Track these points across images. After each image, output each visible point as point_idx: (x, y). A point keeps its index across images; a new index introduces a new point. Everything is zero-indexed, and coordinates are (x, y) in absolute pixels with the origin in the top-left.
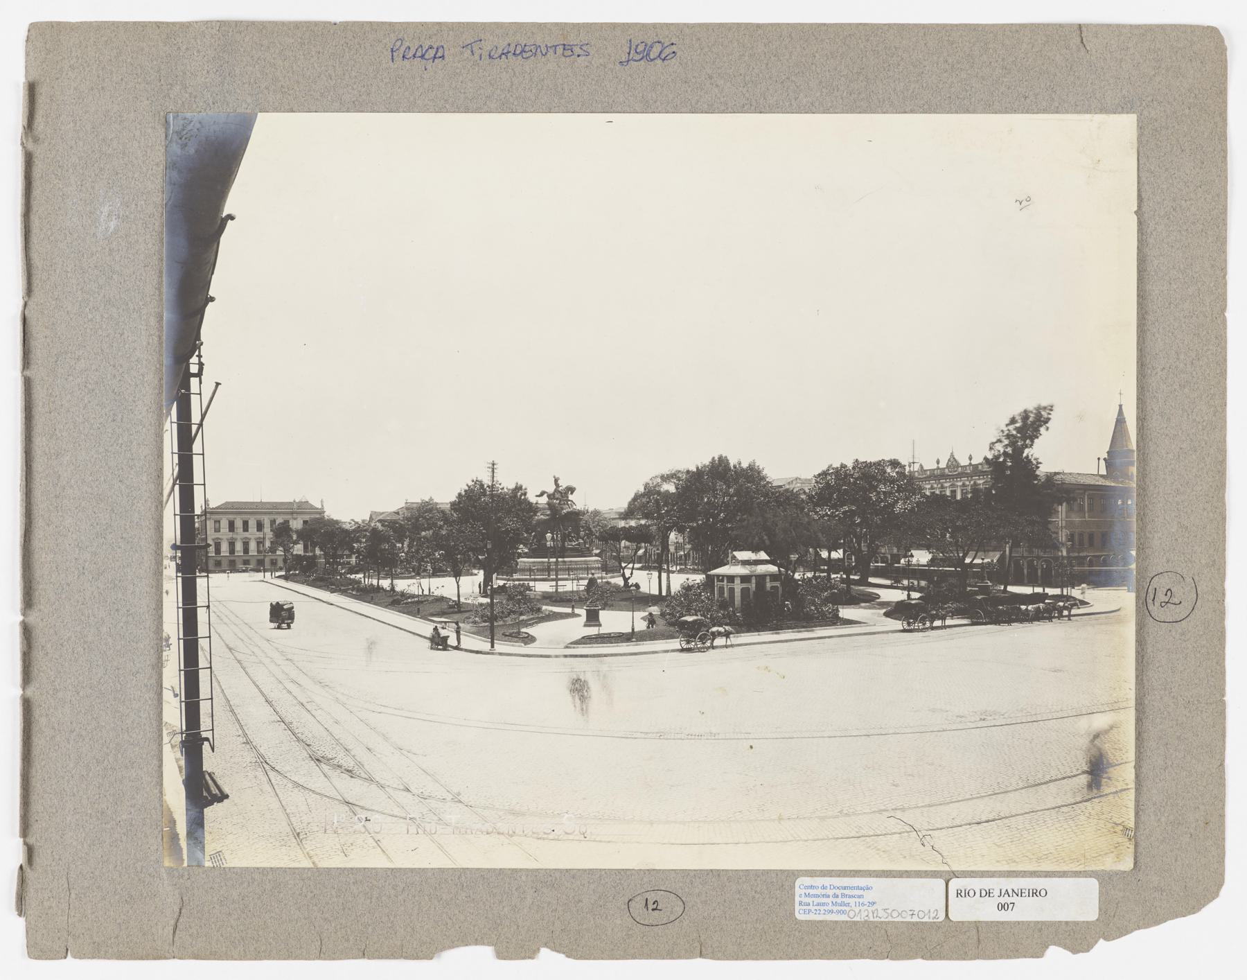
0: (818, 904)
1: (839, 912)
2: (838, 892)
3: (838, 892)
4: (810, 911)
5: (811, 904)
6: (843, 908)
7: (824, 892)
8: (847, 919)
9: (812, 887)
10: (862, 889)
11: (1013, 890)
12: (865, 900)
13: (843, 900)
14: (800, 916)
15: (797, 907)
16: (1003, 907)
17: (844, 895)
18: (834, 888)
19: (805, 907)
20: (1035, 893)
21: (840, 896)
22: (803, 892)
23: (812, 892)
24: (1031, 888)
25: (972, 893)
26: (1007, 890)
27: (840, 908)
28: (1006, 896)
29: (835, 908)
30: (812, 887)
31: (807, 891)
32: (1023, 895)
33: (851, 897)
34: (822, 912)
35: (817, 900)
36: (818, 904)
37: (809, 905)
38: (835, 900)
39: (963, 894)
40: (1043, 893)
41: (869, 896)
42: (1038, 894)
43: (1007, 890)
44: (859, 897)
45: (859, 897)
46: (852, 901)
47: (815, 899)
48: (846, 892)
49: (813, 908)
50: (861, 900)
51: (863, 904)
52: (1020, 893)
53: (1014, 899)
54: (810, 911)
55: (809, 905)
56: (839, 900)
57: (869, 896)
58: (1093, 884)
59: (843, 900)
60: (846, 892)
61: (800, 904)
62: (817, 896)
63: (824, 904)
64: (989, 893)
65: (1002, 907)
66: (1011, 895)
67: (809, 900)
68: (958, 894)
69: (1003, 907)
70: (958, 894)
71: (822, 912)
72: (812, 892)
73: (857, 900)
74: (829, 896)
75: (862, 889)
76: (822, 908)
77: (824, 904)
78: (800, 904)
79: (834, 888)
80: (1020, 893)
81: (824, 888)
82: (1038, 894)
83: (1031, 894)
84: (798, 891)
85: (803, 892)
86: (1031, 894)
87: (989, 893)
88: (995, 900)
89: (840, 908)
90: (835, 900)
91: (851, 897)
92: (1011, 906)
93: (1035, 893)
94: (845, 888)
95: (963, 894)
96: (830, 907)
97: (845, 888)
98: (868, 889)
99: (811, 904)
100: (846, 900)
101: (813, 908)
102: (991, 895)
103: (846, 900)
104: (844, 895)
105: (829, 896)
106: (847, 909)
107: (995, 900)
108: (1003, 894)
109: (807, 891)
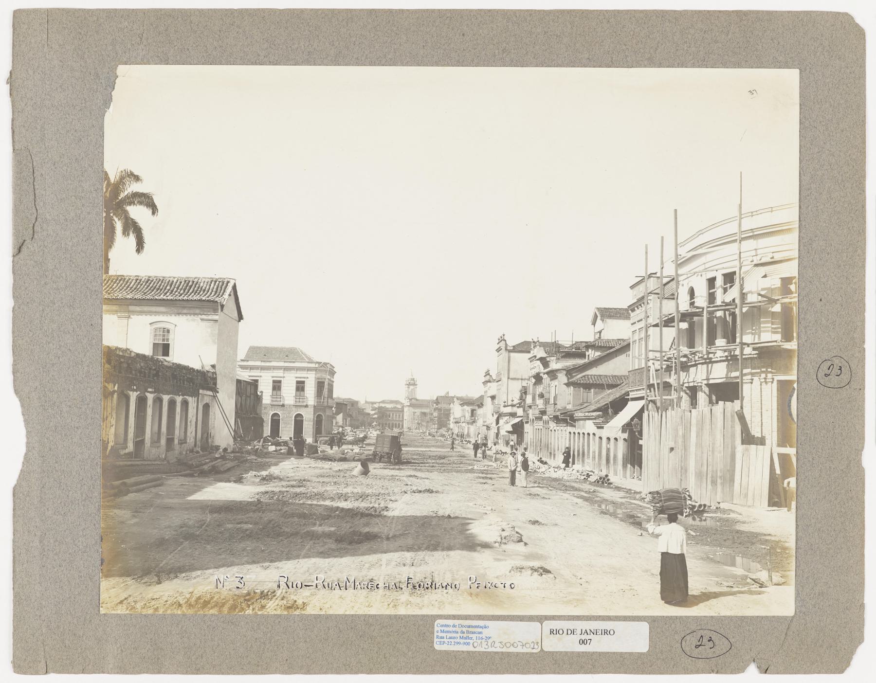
0: (450, 638)
1: (464, 643)
2: (464, 629)
3: (464, 629)
4: (444, 642)
6: (468, 641)
7: (454, 629)
8: (471, 648)
10: (481, 627)
11: (591, 631)
12: (483, 636)
13: (467, 635)
14: (437, 647)
15: (436, 640)
16: (583, 642)
17: (468, 632)
18: (462, 626)
19: (442, 640)
20: (606, 632)
22: (439, 629)
23: (446, 629)
24: (603, 629)
25: (561, 632)
26: (586, 630)
27: (465, 641)
28: (586, 634)
29: (462, 641)
30: (447, 626)
31: (442, 629)
32: (598, 633)
33: (473, 633)
34: (453, 643)
35: (449, 635)
36: (450, 638)
37: (443, 638)
39: (555, 632)
40: (612, 632)
41: (486, 633)
42: (608, 633)
43: (586, 630)
44: (480, 633)
45: (480, 633)
46: (474, 636)
47: (447, 634)
49: (445, 640)
50: (481, 636)
52: (595, 633)
53: (591, 636)
54: (444, 642)
55: (443, 638)
56: (465, 635)
57: (486, 633)
58: (645, 627)
59: (467, 635)
60: (470, 630)
61: (437, 637)
62: (450, 632)
63: (454, 638)
64: (573, 632)
65: (583, 642)
66: (589, 633)
67: (444, 635)
68: (552, 632)
69: (583, 642)
70: (552, 632)
71: (453, 643)
72: (446, 629)
73: (479, 635)
75: (481, 627)
76: (452, 640)
77: (454, 638)
78: (437, 637)
79: (462, 626)
80: (595, 633)
81: (454, 626)
82: (608, 633)
83: (603, 633)
84: (436, 628)
85: (439, 629)
86: (603, 633)
87: (573, 632)
88: (576, 638)
89: (465, 641)
90: (462, 635)
92: (589, 641)
93: (606, 632)
95: (555, 632)
96: (458, 640)
97: (469, 627)
98: (485, 627)
100: (471, 636)
101: (445, 640)
102: (575, 633)
104: (468, 632)
106: (471, 642)
107: (576, 638)
108: (583, 633)
109: (442, 629)
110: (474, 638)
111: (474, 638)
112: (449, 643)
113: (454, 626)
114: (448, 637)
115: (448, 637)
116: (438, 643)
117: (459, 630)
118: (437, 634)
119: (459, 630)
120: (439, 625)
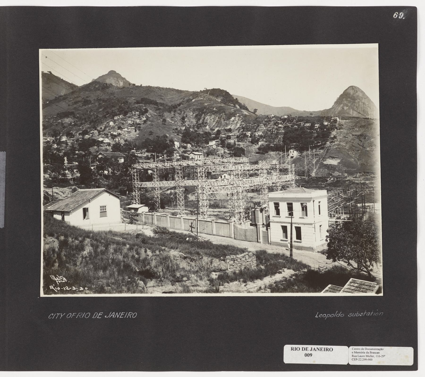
0: (360, 356)
2: (369, 351)
3: (369, 351)
4: (357, 359)
5: (357, 356)
7: (362, 351)
9: (358, 349)
10: (379, 349)
17: (371, 352)
21: (369, 353)
23: (358, 351)
29: (367, 358)
30: (358, 349)
33: (373, 353)
34: (362, 360)
35: (360, 354)
36: (360, 356)
37: (356, 356)
38: (367, 354)
44: (378, 353)
45: (378, 353)
46: (375, 355)
48: (372, 351)
49: (357, 358)
50: (379, 354)
51: (379, 356)
54: (357, 359)
56: (369, 355)
59: (371, 354)
60: (372, 351)
61: (353, 356)
63: (362, 356)
67: (356, 354)
71: (362, 360)
74: (364, 353)
75: (379, 349)
76: (362, 358)
77: (362, 356)
90: (367, 354)
91: (375, 353)
94: (371, 349)
96: (365, 358)
97: (371, 349)
98: (381, 349)
99: (357, 356)
100: (372, 355)
101: (357, 358)
103: (372, 355)
104: (371, 352)
105: (364, 353)
109: (355, 351)
110: (375, 356)
111: (375, 356)
112: (360, 360)
113: (363, 349)
114: (359, 356)
115: (359, 356)
116: (353, 359)
117: (366, 351)
118: (352, 354)
119: (366, 351)
120: (353, 349)
